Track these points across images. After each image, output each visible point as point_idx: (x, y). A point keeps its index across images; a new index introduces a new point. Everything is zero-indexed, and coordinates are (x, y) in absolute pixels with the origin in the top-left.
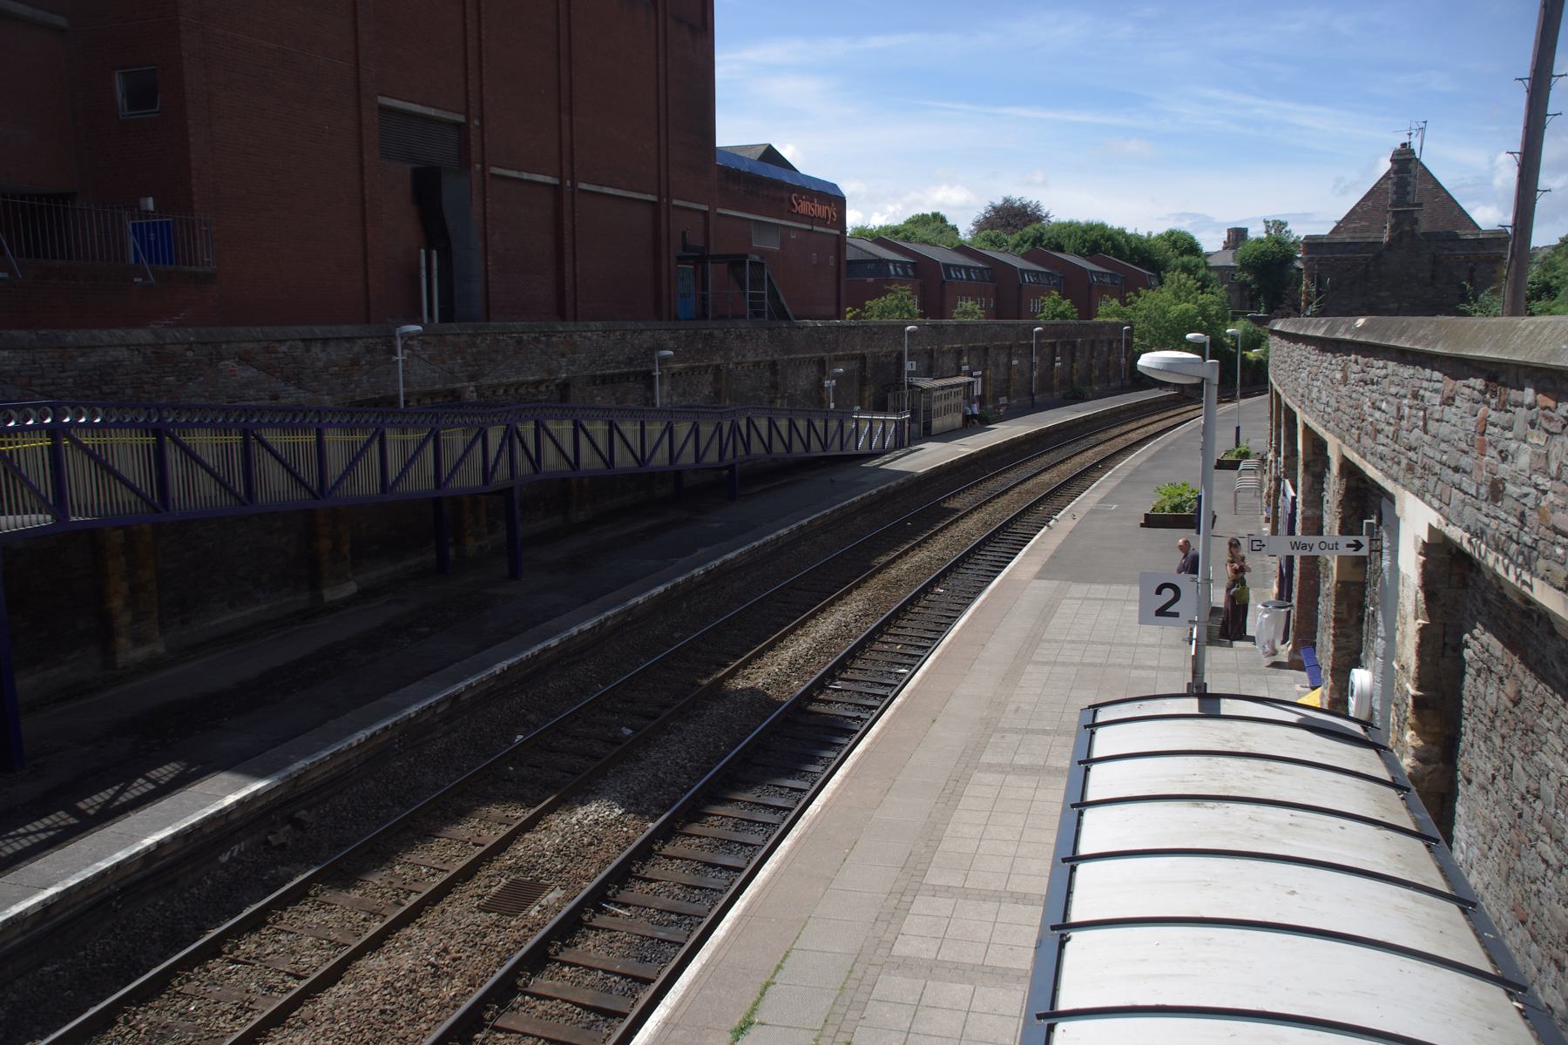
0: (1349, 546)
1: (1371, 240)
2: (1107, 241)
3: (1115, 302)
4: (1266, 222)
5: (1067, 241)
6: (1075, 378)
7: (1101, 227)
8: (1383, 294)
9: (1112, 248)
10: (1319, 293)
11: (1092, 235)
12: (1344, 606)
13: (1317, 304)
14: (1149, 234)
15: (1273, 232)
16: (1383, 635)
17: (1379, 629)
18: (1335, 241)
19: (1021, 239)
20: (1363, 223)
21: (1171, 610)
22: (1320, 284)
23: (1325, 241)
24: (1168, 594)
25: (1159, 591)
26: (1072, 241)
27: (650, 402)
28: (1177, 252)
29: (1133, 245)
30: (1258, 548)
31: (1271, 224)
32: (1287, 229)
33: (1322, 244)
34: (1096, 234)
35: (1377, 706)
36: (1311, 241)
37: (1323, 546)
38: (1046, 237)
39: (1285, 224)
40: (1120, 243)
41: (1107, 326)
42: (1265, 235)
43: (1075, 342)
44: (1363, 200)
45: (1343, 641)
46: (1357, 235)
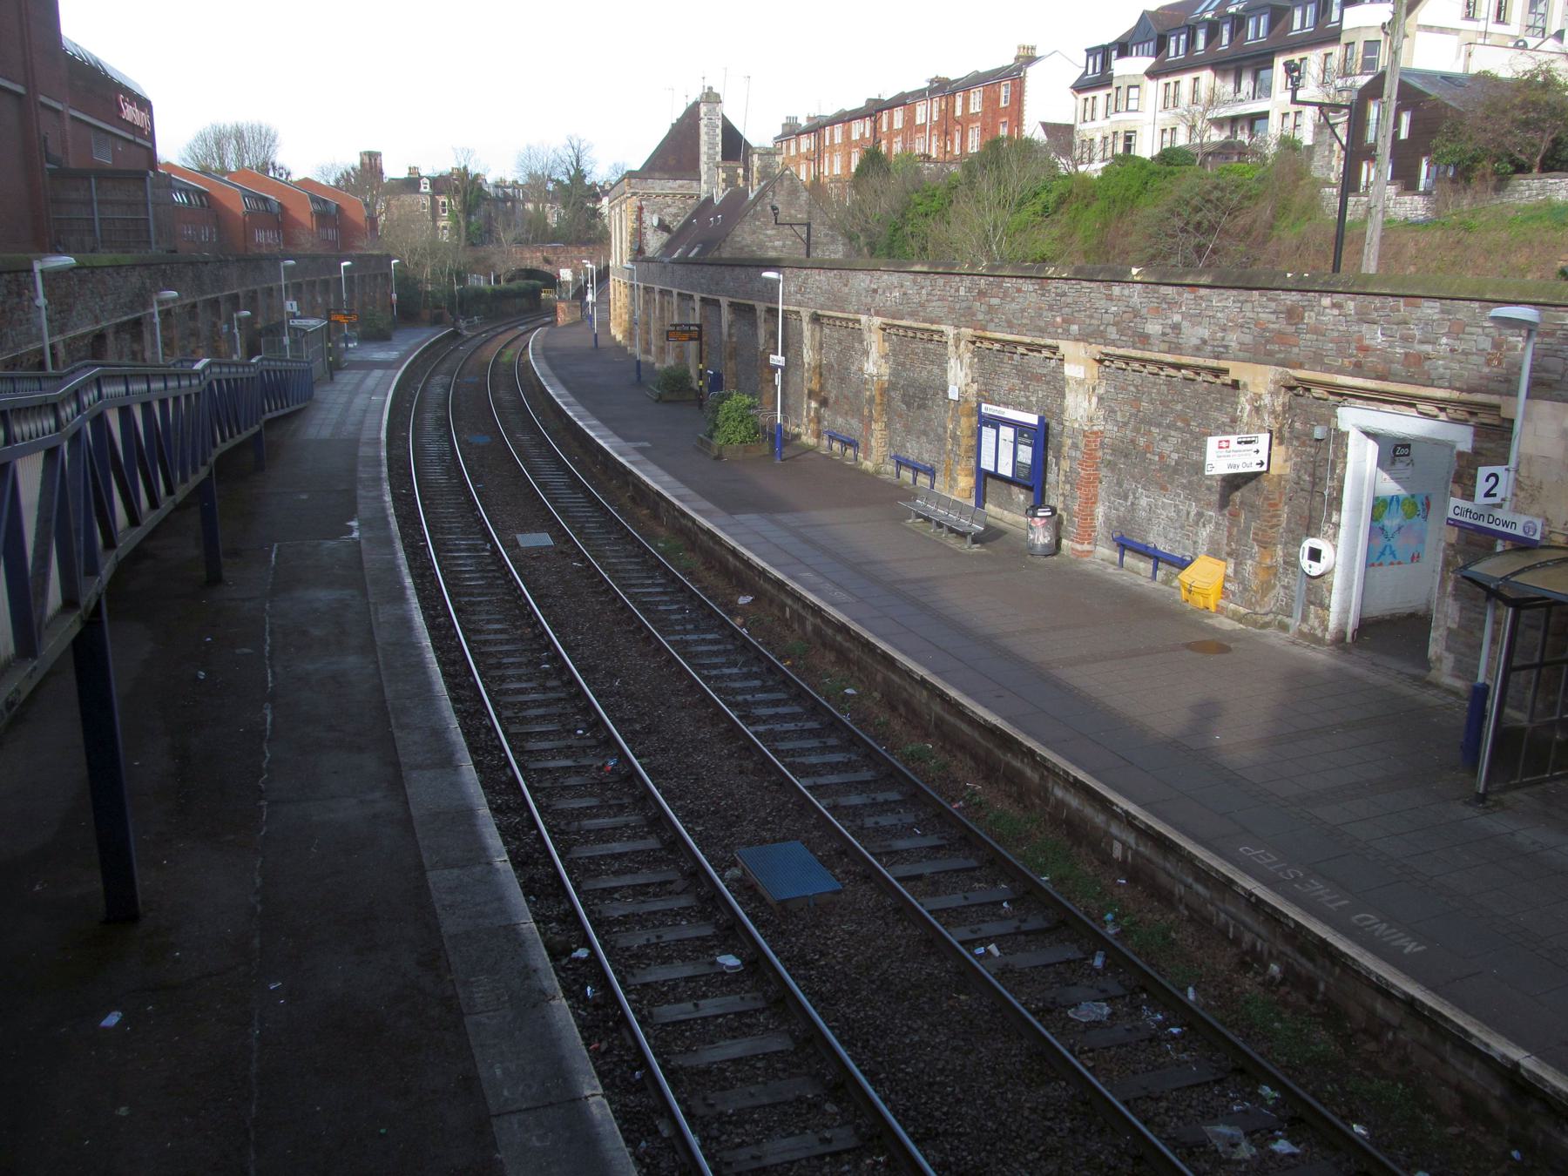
8: (769, 232)
21: (1492, 492)
24: (1492, 480)
25: (1487, 480)
27: (139, 356)
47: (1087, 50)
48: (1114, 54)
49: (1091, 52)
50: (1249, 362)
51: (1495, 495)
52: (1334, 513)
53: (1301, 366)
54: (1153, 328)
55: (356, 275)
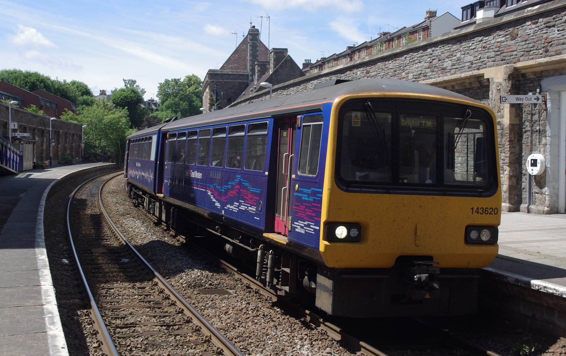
0: (535, 99)
2: (40, 83)
3: (70, 113)
4: (125, 80)
5: (14, 81)
6: (59, 154)
7: (36, 75)
10: (217, 100)
11: (31, 79)
12: (513, 134)
13: (217, 105)
14: (65, 81)
15: (129, 86)
16: (550, 135)
17: (547, 133)
18: (224, 73)
20: (236, 65)
22: (217, 95)
23: (219, 73)
26: (18, 82)
29: (56, 87)
30: (505, 100)
31: (127, 82)
33: (217, 74)
34: (33, 78)
35: (549, 166)
36: (212, 72)
37: (527, 99)
39: (134, 82)
40: (49, 85)
42: (125, 87)
43: (59, 132)
44: (233, 53)
45: (513, 149)
46: (234, 71)
47: (462, 8)
48: (478, 8)
49: (464, 9)
50: (493, 66)
52: (543, 139)
53: (519, 61)
54: (448, 64)
55: (61, 131)
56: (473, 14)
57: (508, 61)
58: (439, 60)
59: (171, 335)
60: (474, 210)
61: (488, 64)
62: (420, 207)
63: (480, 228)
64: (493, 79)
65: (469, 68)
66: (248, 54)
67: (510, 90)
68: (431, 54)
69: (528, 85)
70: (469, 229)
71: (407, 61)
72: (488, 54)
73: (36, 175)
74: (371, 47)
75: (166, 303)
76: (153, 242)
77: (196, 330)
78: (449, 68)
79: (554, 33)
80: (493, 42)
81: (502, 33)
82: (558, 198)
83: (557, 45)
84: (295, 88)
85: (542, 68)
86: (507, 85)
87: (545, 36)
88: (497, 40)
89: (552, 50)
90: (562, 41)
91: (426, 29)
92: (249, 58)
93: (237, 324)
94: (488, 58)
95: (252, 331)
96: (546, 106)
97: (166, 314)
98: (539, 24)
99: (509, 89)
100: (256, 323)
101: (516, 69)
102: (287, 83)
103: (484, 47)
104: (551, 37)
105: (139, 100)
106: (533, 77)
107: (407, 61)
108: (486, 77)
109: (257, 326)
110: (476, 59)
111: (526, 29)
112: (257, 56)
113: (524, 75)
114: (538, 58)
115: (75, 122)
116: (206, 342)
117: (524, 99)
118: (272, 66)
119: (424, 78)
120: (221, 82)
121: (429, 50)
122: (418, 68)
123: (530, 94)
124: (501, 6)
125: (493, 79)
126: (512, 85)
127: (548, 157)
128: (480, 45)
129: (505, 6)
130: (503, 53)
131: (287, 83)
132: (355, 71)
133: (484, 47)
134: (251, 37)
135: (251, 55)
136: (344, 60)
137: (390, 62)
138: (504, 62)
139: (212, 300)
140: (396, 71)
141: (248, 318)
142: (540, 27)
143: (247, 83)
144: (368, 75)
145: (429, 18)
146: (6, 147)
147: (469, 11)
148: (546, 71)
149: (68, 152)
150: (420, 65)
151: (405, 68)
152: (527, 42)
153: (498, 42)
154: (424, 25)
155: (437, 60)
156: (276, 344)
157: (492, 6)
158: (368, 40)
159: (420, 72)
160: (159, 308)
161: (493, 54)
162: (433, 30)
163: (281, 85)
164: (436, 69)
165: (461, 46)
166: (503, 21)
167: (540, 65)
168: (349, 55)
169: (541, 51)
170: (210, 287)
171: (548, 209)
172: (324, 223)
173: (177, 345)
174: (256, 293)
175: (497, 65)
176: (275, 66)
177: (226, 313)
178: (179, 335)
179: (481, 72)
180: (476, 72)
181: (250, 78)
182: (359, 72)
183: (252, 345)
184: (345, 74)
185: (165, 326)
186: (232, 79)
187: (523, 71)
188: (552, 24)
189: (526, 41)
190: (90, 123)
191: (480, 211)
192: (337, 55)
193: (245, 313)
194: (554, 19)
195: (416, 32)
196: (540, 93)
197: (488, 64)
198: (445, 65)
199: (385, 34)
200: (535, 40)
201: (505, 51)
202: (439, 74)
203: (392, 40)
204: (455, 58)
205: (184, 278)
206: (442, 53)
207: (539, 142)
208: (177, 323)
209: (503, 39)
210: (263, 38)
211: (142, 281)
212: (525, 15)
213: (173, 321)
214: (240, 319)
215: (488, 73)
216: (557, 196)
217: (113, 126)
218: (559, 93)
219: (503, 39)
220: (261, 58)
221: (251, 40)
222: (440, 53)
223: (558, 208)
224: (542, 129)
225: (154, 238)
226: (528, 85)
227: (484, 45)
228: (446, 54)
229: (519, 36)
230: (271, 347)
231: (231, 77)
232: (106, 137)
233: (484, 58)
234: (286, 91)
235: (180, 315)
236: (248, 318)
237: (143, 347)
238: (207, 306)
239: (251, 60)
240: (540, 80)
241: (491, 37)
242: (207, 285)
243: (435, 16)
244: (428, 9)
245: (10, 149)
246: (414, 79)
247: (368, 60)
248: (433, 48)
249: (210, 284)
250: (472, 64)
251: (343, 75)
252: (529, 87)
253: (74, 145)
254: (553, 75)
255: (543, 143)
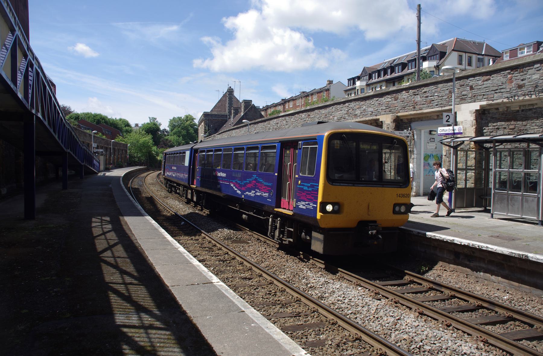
1: (223, 114)
2: (102, 120)
3: (121, 137)
4: (150, 118)
5: (88, 119)
6: (115, 161)
7: (100, 115)
9: (105, 122)
10: (209, 130)
14: (116, 119)
15: (152, 121)
19: (70, 118)
21: (448, 121)
24: (448, 117)
25: (446, 117)
26: (90, 119)
28: (124, 125)
29: (111, 122)
32: (157, 120)
35: (415, 170)
38: (80, 117)
39: (156, 119)
40: (107, 121)
41: (122, 145)
42: (150, 122)
43: (115, 148)
44: (218, 103)
47: (348, 79)
48: (356, 80)
49: (349, 80)
50: (385, 114)
51: (449, 122)
52: (412, 155)
53: (399, 112)
54: (358, 112)
56: (354, 83)
57: (393, 112)
58: (353, 110)
59: (227, 266)
60: (398, 195)
61: (382, 113)
62: (371, 193)
63: (400, 205)
64: (384, 121)
65: (371, 115)
66: (227, 103)
67: (394, 128)
68: (348, 106)
69: (404, 126)
70: (395, 205)
71: (334, 110)
72: (382, 108)
73: (108, 174)
74: (296, 99)
75: (214, 248)
76: (191, 213)
77: (241, 264)
78: (359, 114)
79: (418, 98)
80: (384, 101)
81: (389, 96)
82: (419, 188)
83: (420, 105)
84: (262, 124)
85: (412, 117)
86: (393, 125)
87: (413, 99)
88: (387, 100)
89: (417, 107)
90: (423, 103)
91: (328, 90)
92: (227, 105)
93: (263, 260)
94: (382, 110)
95: (274, 263)
96: (414, 137)
97: (218, 255)
98: (409, 93)
99: (394, 127)
100: (275, 259)
101: (397, 116)
102: (257, 121)
103: (379, 104)
104: (416, 100)
105: (158, 129)
106: (406, 121)
107: (334, 110)
108: (380, 120)
109: (276, 261)
110: (374, 110)
111: (403, 95)
112: (232, 104)
113: (402, 120)
114: (410, 111)
115: (123, 142)
116: (249, 270)
117: (403, 134)
118: (243, 110)
119: (344, 119)
120: (210, 119)
121: (347, 104)
122: (340, 114)
123: (405, 130)
124: (369, 79)
125: (384, 121)
126: (396, 125)
127: (415, 165)
128: (377, 103)
129: (371, 79)
130: (390, 107)
131: (257, 121)
132: (301, 114)
133: (379, 104)
134: (229, 93)
135: (228, 103)
136: (280, 107)
137: (323, 110)
138: (391, 112)
139: (243, 247)
140: (326, 115)
141: (269, 256)
142: (410, 95)
143: (226, 120)
144: (309, 117)
145: (329, 84)
146: (93, 158)
147: (352, 81)
148: (414, 118)
149: (120, 160)
150: (341, 112)
151: (332, 114)
152: (403, 102)
153: (387, 101)
154: (326, 88)
155: (351, 110)
156: (292, 271)
157: (364, 79)
158: (294, 96)
159: (341, 116)
160: (212, 251)
161: (384, 108)
162: (331, 91)
163: (253, 122)
164: (351, 115)
165: (366, 103)
166: (390, 90)
167: (411, 115)
168: (282, 104)
169: (411, 108)
170: (236, 239)
171: (415, 194)
172: (320, 203)
173: (234, 272)
174: (264, 242)
175: (387, 114)
176: (245, 110)
177: (254, 254)
178: (231, 266)
179: (378, 117)
180: (375, 118)
181: (228, 117)
182: (303, 115)
183: (277, 271)
184: (295, 116)
185: (221, 261)
186: (218, 117)
187: (402, 118)
188: (417, 93)
189: (403, 101)
190: (132, 143)
191: (401, 196)
192: (276, 104)
193: (266, 254)
194: (418, 91)
195: (322, 92)
196: (410, 130)
197: (382, 113)
198: (356, 113)
199: (303, 92)
200: (408, 102)
201: (391, 106)
202: (353, 118)
203: (308, 96)
204: (362, 109)
205: (220, 234)
206: (355, 106)
207: (410, 157)
208: (227, 260)
209: (390, 100)
210: (236, 94)
211: (195, 235)
212: (402, 87)
213: (225, 259)
214: (264, 257)
215: (382, 118)
216: (419, 187)
217: (145, 145)
218: (420, 131)
219: (390, 100)
220: (235, 106)
221: (229, 95)
222: (353, 106)
223: (419, 193)
224: (412, 150)
225: (191, 211)
226: (404, 126)
227: (379, 102)
228: (357, 107)
229: (399, 99)
230: (289, 272)
231: (217, 116)
232: (141, 150)
233: (380, 110)
234: (256, 125)
235: (227, 255)
236: (269, 256)
237: (216, 273)
238: (241, 250)
239: (228, 107)
240: (411, 123)
241: (383, 99)
242: (234, 238)
243: (332, 83)
244: (328, 79)
245: (95, 159)
246: (338, 120)
247: (309, 108)
248: (349, 103)
249: (236, 238)
250: (372, 113)
251: (293, 117)
252: (405, 127)
253: (123, 156)
254: (417, 121)
255: (412, 158)
